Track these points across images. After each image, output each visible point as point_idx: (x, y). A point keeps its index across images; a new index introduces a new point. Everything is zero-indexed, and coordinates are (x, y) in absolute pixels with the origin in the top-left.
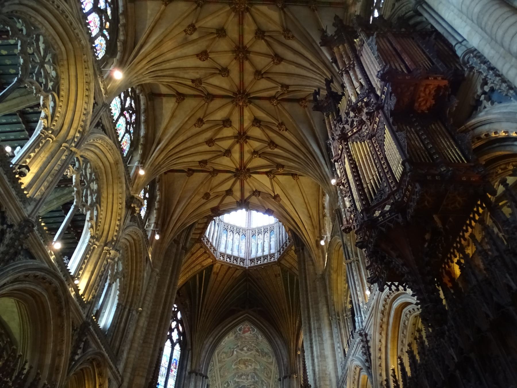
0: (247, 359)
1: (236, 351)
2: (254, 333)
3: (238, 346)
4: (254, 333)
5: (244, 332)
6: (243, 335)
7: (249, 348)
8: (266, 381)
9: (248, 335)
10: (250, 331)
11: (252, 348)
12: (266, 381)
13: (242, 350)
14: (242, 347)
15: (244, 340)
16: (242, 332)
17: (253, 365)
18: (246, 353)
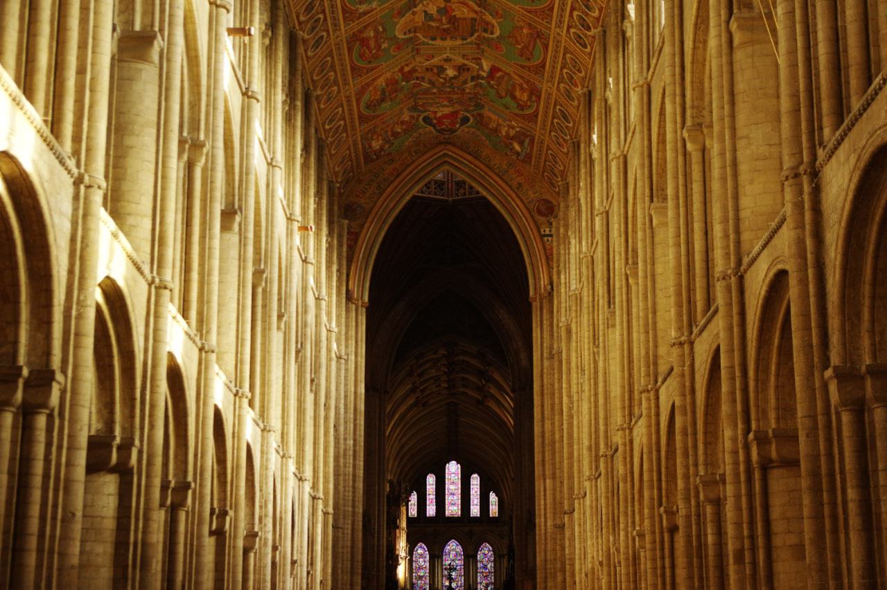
0: (443, 39)
1: (483, 71)
2: (426, 114)
3: (473, 79)
4: (426, 114)
5: (454, 115)
6: (457, 107)
7: (439, 76)
8: (363, 8)
9: (441, 109)
10: (436, 118)
11: (428, 76)
12: (363, 8)
13: (462, 69)
14: (462, 79)
15: (455, 97)
16: (460, 116)
17: (420, 18)
18: (447, 60)
